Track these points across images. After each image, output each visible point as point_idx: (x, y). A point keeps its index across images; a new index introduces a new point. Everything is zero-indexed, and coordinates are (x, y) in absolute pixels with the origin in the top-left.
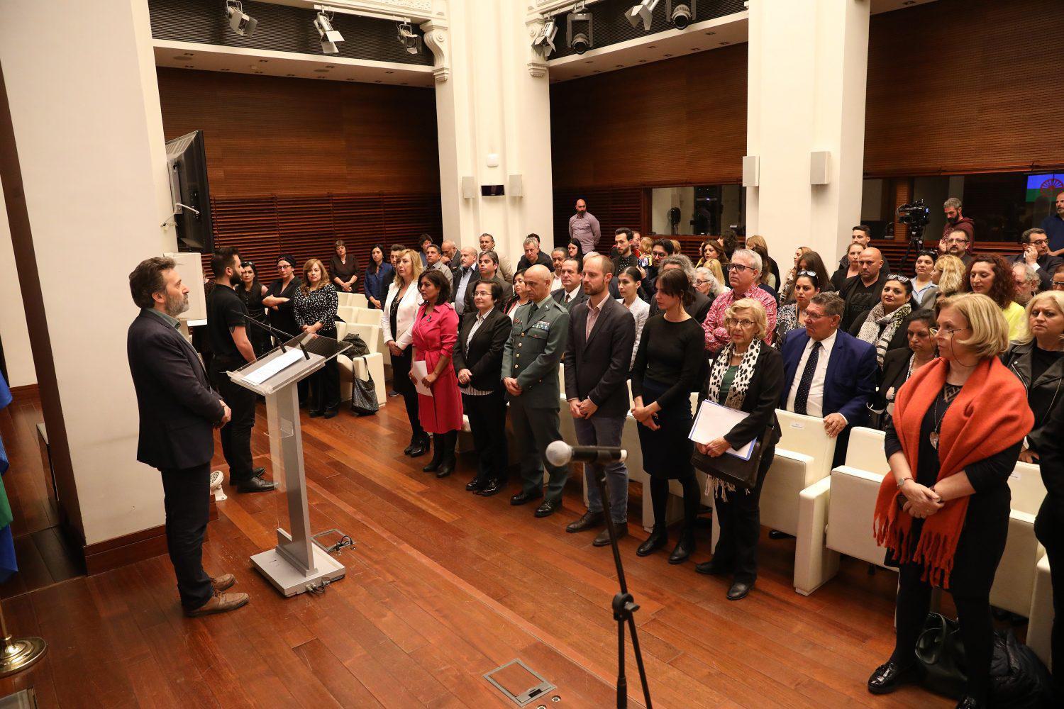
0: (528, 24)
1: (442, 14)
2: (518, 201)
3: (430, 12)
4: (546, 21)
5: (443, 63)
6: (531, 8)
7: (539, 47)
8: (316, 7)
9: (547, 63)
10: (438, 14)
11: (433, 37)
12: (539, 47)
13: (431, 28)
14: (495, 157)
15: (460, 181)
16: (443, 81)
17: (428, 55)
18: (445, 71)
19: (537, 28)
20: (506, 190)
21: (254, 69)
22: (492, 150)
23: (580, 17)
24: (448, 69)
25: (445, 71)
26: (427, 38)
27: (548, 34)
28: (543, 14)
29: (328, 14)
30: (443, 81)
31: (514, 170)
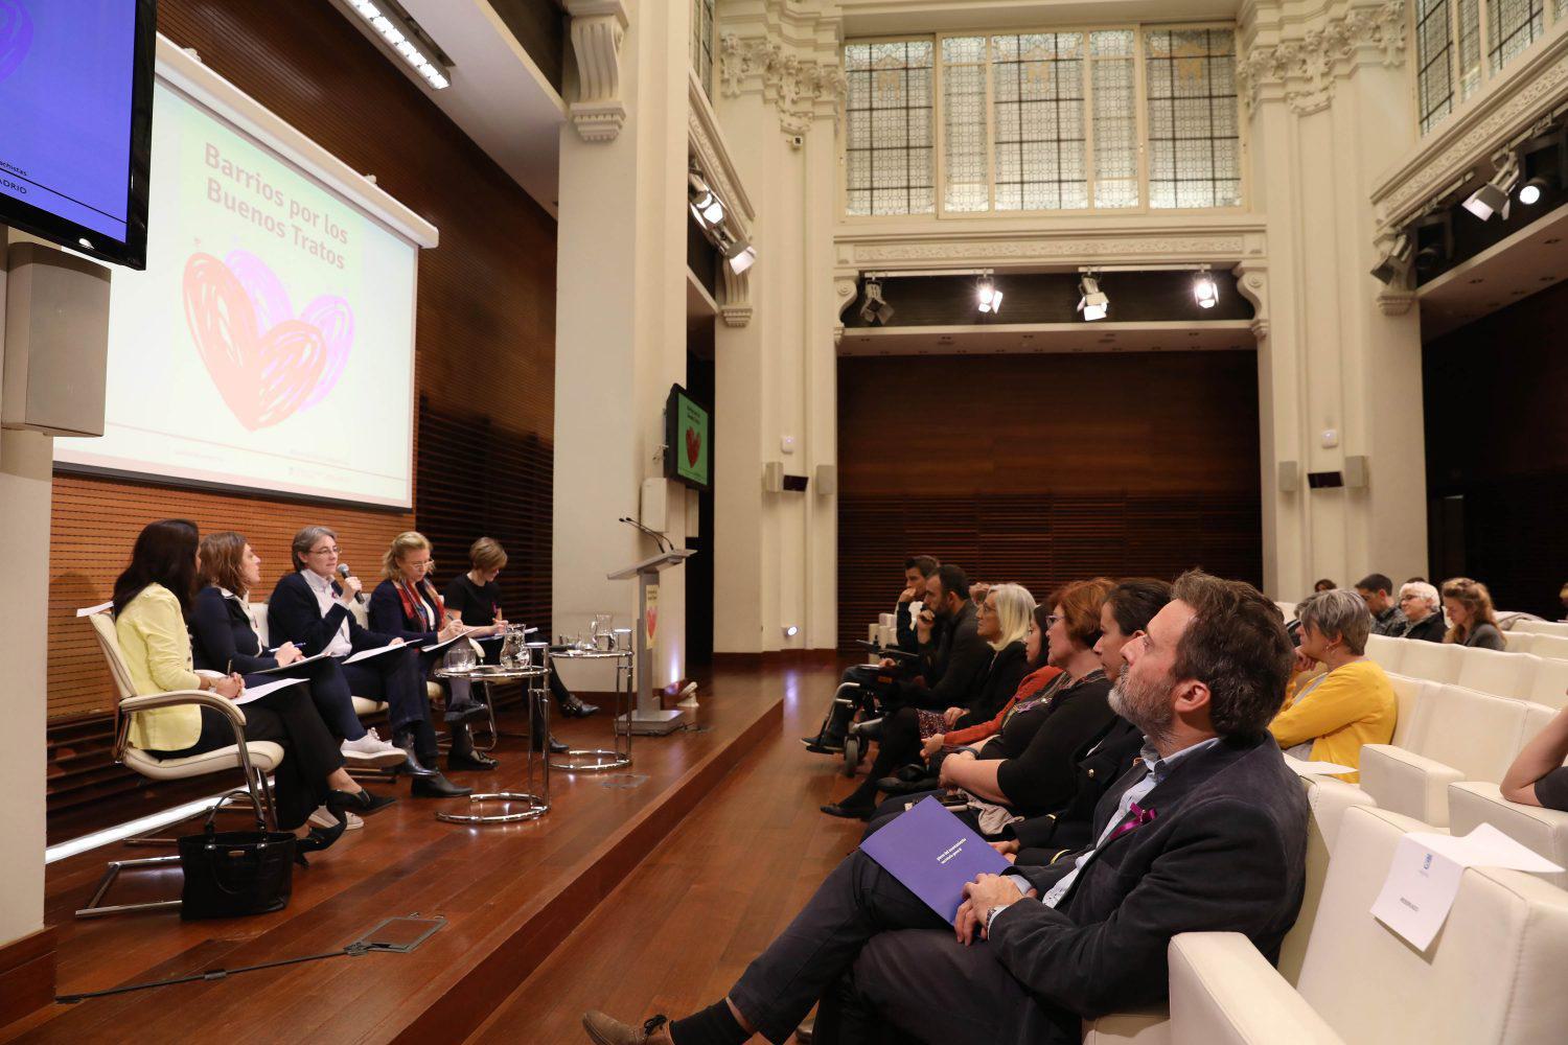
0: (1377, 243)
1: (1258, 252)
2: (1362, 493)
3: (1241, 252)
4: (1397, 236)
5: (1262, 315)
6: (1379, 222)
7: (1384, 272)
8: (1081, 270)
9: (1411, 293)
10: (1253, 252)
11: (1246, 283)
12: (1384, 272)
13: (1242, 272)
14: (1330, 434)
15: (1277, 466)
16: (1264, 337)
17: (1237, 303)
18: (1262, 324)
19: (1386, 247)
20: (1344, 476)
21: (1026, 348)
22: (1329, 424)
23: (1432, 221)
24: (1265, 321)
25: (1262, 324)
26: (1239, 285)
27: (1395, 253)
28: (1394, 226)
29: (1095, 275)
30: (1264, 337)
31: (1359, 446)
